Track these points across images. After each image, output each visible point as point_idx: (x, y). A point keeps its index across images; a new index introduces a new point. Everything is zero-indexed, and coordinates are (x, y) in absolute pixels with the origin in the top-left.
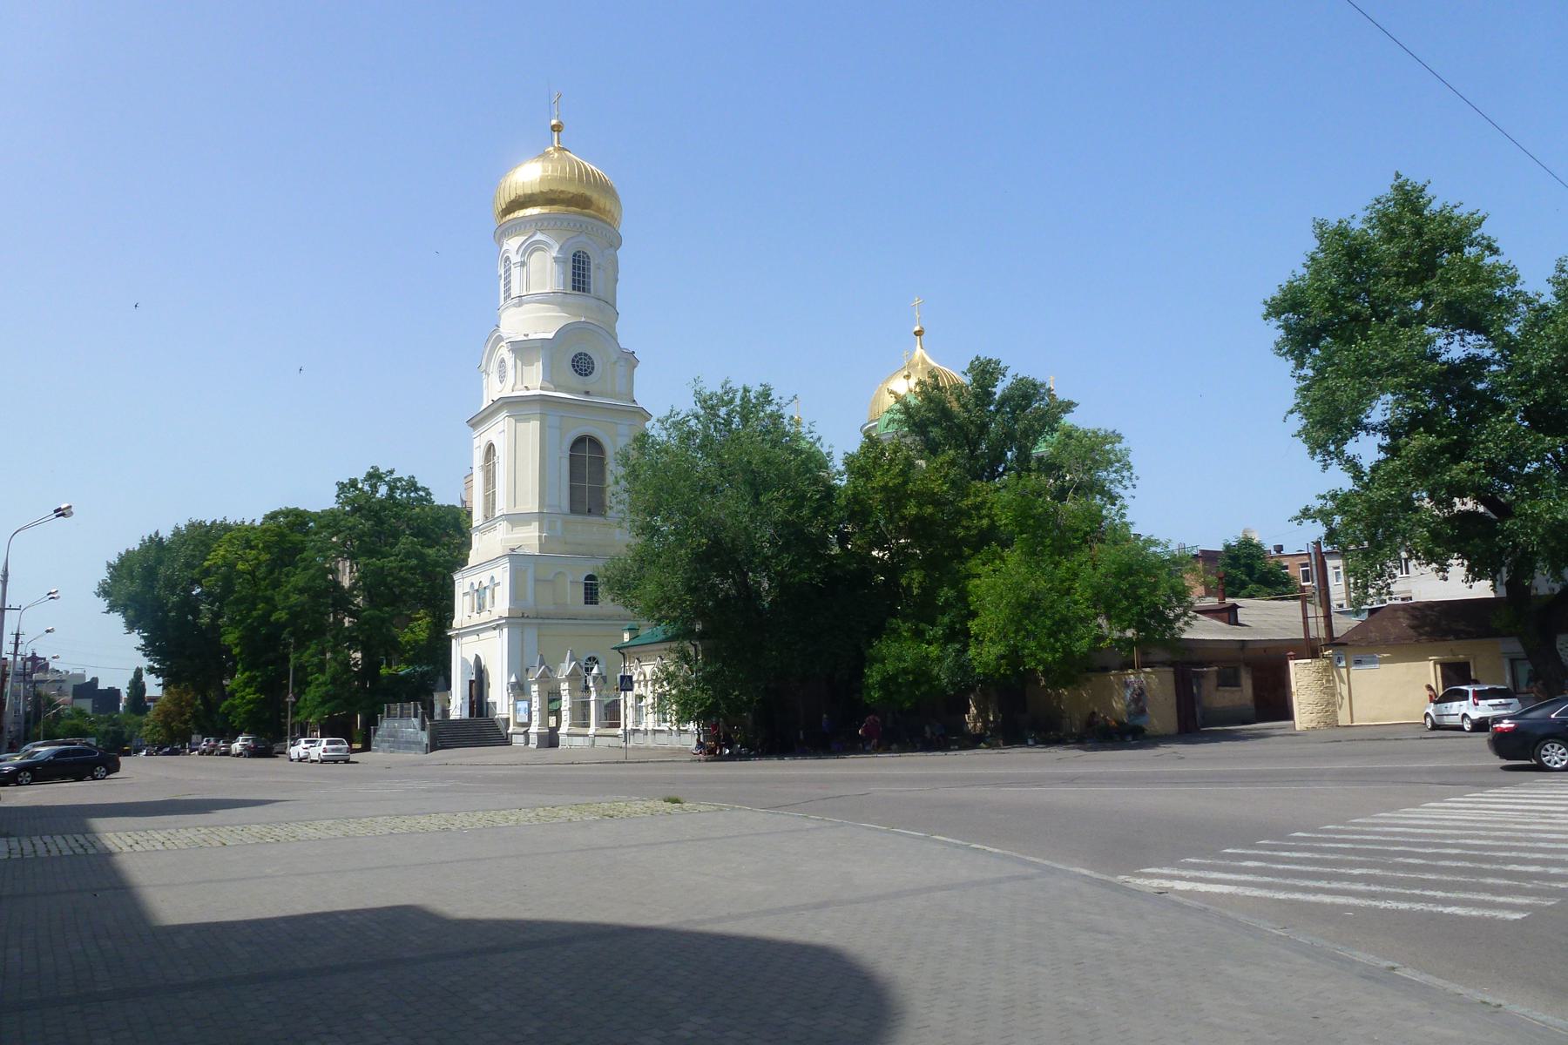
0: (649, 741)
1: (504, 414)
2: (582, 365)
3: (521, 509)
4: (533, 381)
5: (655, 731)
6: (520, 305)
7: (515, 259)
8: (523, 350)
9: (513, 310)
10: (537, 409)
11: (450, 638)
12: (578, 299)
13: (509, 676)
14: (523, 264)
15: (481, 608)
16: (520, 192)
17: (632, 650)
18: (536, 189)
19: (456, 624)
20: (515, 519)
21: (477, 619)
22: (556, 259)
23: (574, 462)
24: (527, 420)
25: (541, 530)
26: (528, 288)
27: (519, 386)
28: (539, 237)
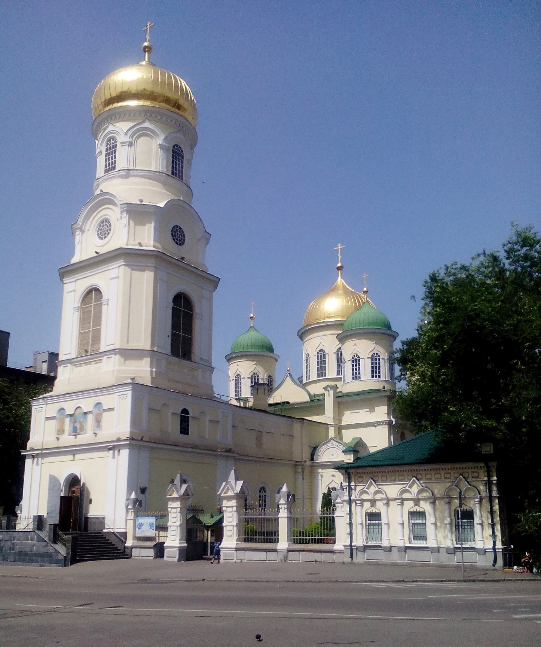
0: (395, 557)
1: (121, 262)
2: (178, 236)
3: (133, 345)
4: (147, 238)
5: (407, 548)
6: (127, 177)
7: (121, 138)
8: (137, 212)
9: (120, 180)
10: (152, 262)
11: (24, 457)
12: (173, 181)
13: (129, 493)
14: (131, 144)
15: (75, 432)
16: (125, 89)
17: (360, 470)
18: (141, 87)
19: (30, 445)
20: (127, 354)
21: (67, 440)
22: (161, 147)
23: (175, 313)
24: (142, 269)
25: (151, 367)
26: (135, 164)
27: (131, 241)
28: (147, 124)
